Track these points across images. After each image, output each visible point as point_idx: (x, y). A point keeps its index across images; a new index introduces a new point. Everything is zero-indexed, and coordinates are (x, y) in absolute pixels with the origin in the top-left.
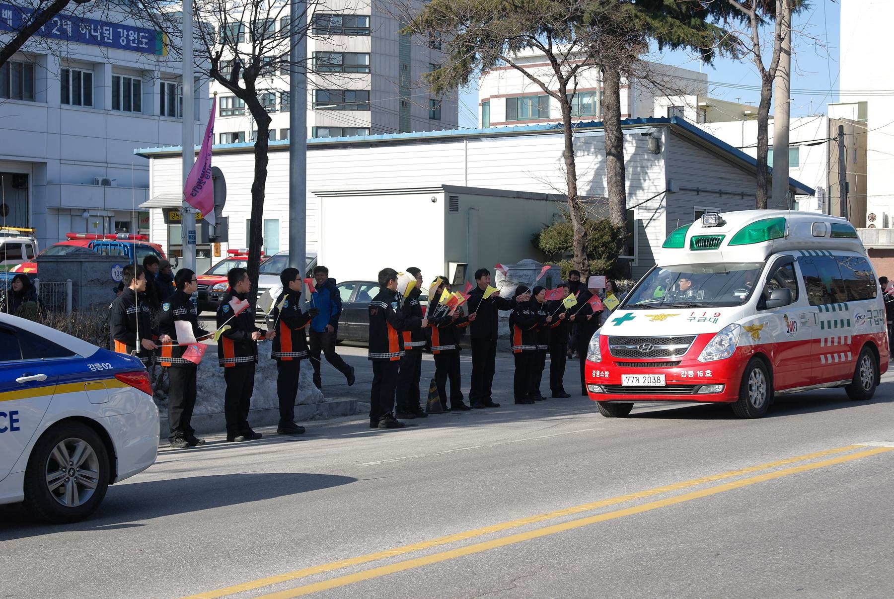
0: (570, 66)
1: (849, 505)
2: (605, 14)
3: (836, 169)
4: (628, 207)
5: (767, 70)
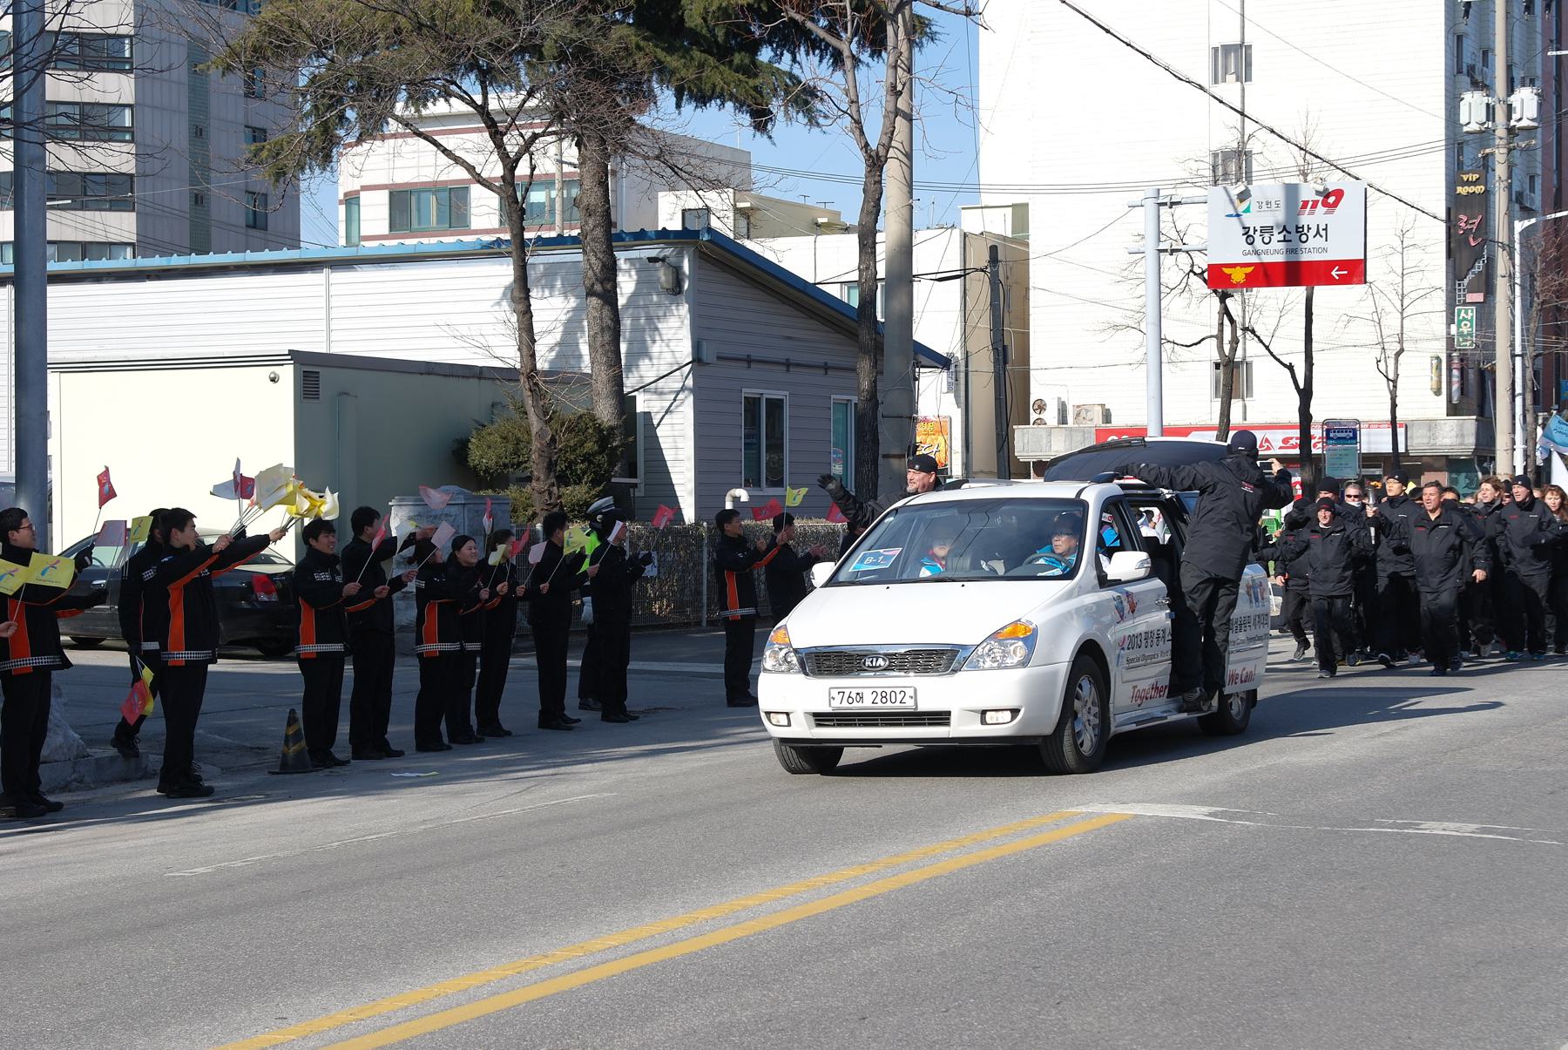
0: (521, 135)
1: (1074, 920)
2: (583, 43)
3: (985, 324)
4: (626, 390)
5: (874, 148)
